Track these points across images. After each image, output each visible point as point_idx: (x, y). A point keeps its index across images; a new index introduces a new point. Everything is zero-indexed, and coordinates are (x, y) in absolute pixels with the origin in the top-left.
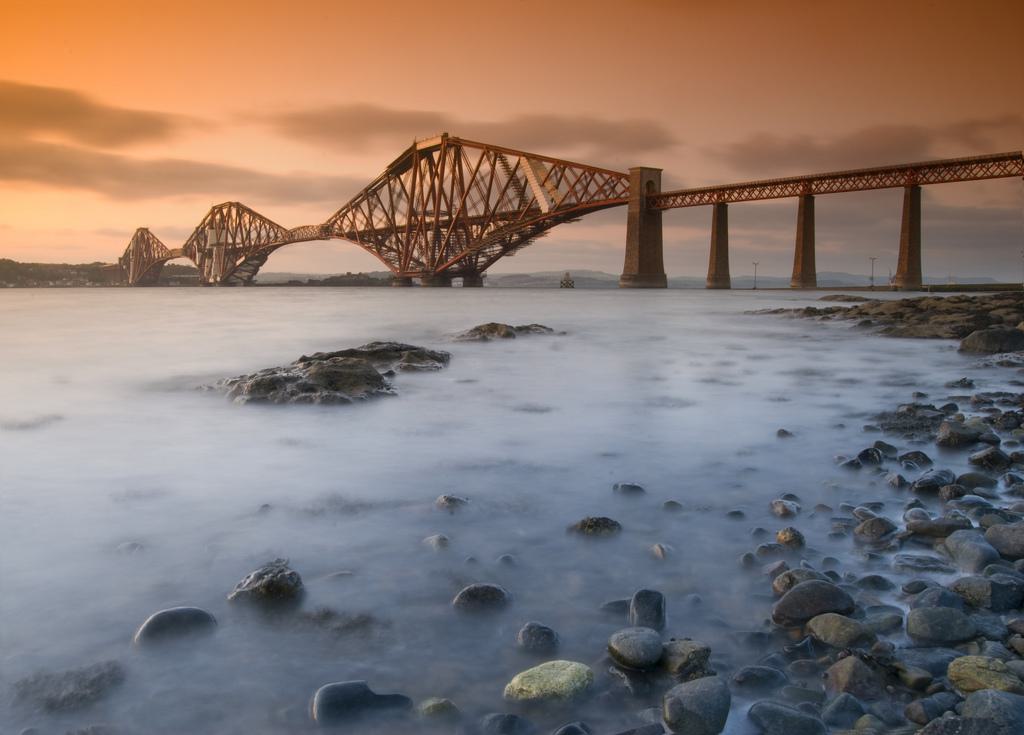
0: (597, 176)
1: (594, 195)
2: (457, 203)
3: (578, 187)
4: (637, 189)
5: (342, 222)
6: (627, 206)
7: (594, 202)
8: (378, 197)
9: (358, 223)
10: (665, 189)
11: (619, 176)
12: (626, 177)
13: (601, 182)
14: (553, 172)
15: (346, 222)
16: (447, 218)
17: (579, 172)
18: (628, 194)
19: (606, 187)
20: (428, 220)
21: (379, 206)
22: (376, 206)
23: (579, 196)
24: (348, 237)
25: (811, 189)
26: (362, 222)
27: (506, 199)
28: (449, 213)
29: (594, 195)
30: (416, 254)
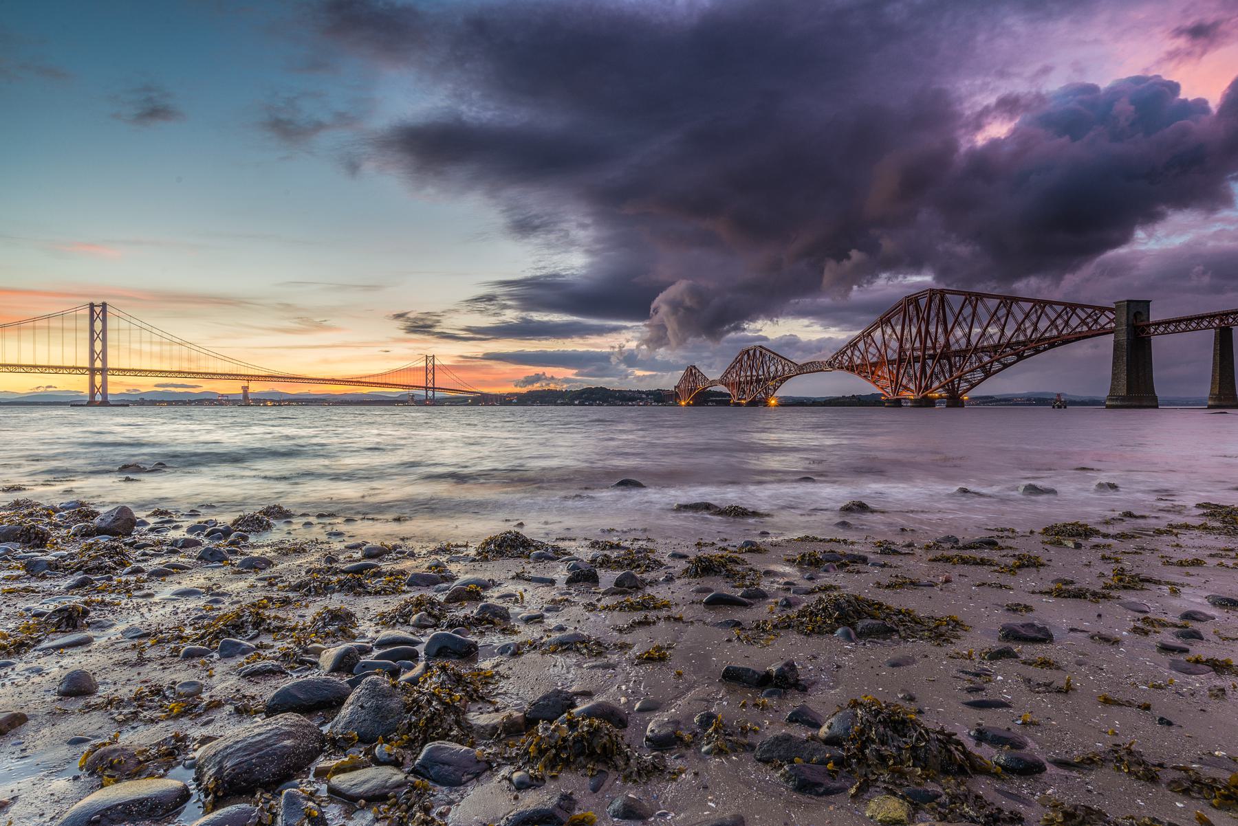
0: (1078, 311)
1: (1076, 327)
2: (942, 340)
4: (1124, 319)
5: (842, 358)
7: (1076, 333)
8: (872, 338)
11: (1103, 310)
12: (1111, 310)
13: (1083, 316)
16: (932, 352)
17: (1059, 308)
18: (1113, 325)
19: (1089, 320)
20: (916, 354)
22: (870, 345)
23: (1060, 328)
24: (848, 369)
26: (858, 358)
28: (934, 348)
29: (1076, 327)
30: (904, 382)
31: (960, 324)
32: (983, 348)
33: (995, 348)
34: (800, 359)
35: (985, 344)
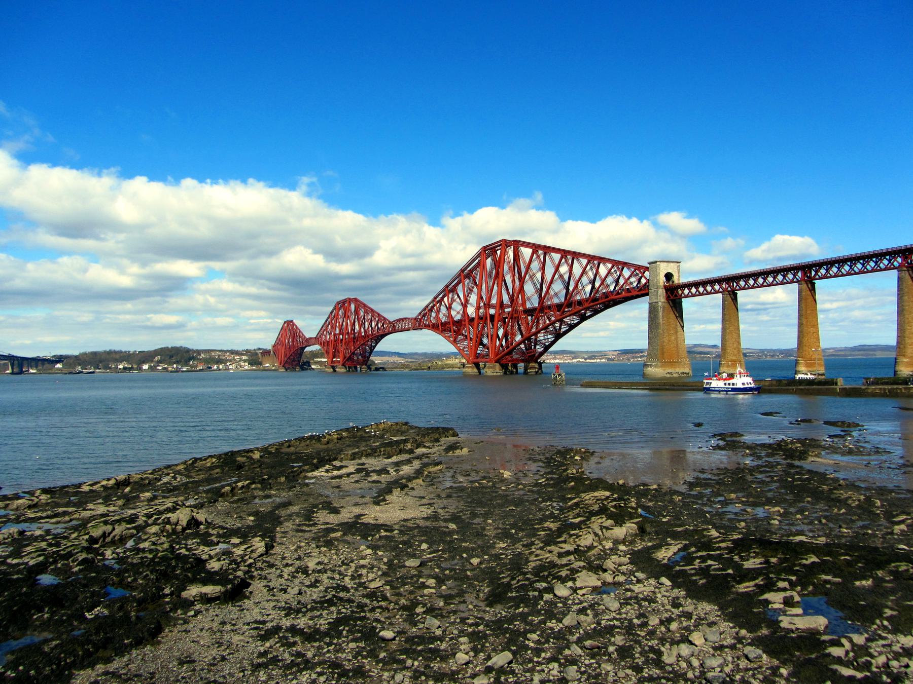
3: (610, 280)
6: (647, 297)
9: (441, 315)
10: (684, 280)
14: (589, 267)
15: (434, 315)
19: (633, 279)
21: (458, 300)
22: (455, 301)
25: (810, 277)
26: (444, 315)
27: (552, 292)
31: (531, 277)
32: (550, 307)
33: (559, 307)
34: (391, 317)
35: (549, 303)
